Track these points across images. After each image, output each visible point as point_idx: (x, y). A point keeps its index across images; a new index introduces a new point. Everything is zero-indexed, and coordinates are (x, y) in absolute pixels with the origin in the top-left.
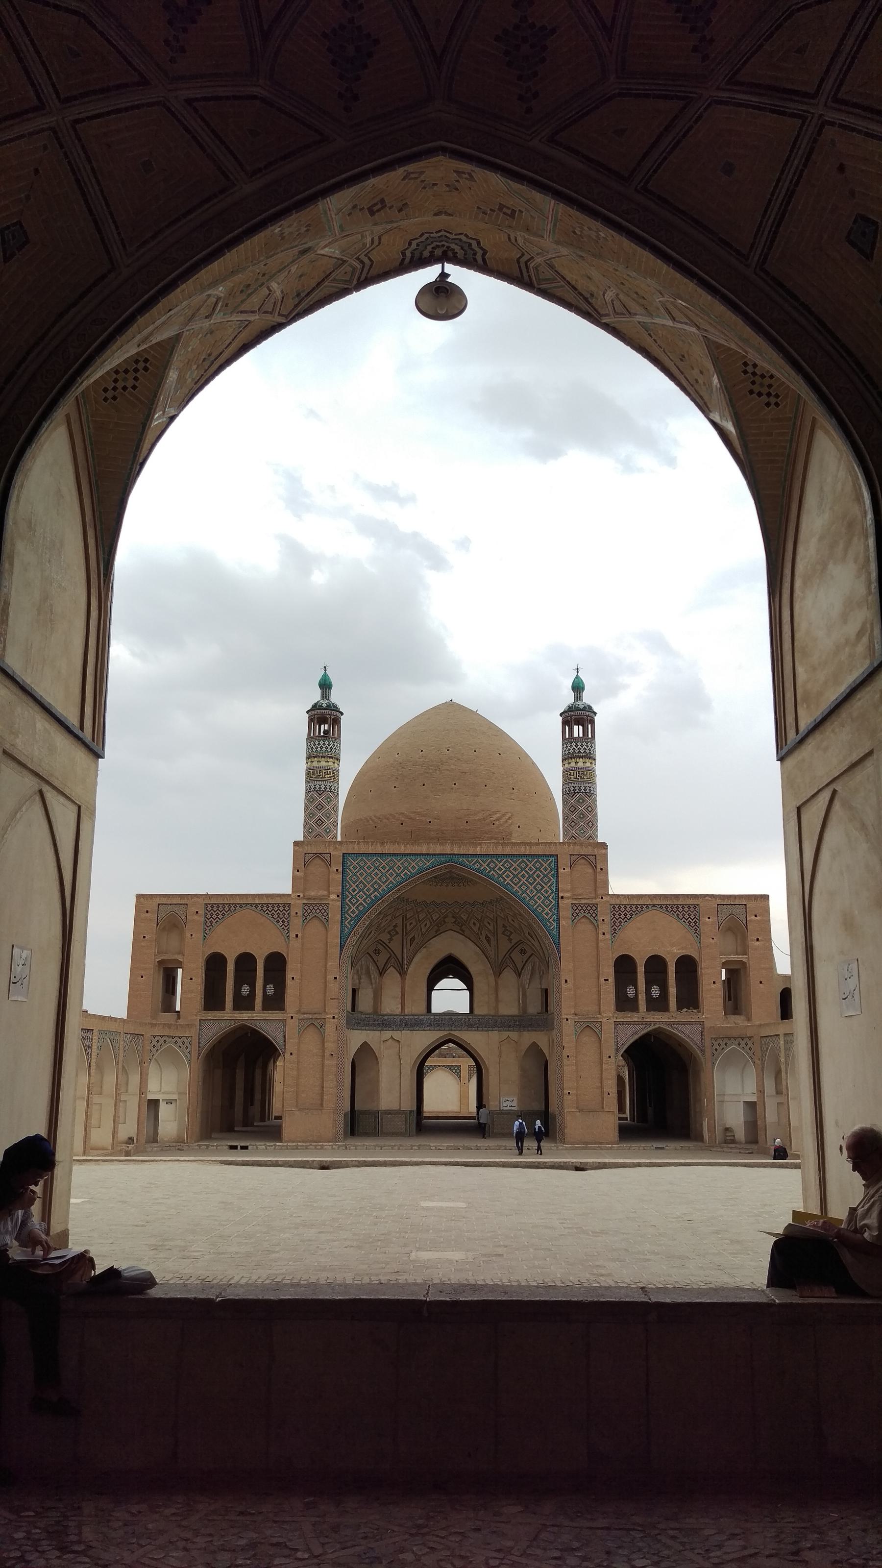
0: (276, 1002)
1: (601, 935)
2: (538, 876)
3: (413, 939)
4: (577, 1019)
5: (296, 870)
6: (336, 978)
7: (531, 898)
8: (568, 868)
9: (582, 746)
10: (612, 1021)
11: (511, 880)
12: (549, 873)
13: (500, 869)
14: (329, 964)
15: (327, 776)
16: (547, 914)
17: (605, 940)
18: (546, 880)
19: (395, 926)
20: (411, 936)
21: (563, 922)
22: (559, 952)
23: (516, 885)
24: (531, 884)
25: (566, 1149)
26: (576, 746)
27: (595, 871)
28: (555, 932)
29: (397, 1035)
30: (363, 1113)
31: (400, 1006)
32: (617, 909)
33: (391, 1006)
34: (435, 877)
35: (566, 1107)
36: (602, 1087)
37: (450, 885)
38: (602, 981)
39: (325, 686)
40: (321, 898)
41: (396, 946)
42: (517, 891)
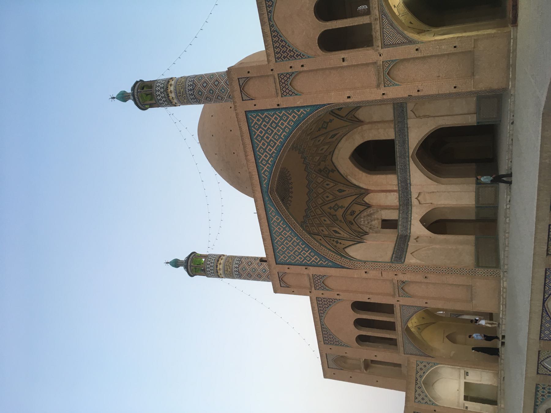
0: (388, 309)
1: (305, 68)
2: (265, 126)
3: (340, 191)
4: (382, 86)
5: (293, 293)
6: (366, 272)
7: (284, 130)
8: (254, 102)
9: (159, 95)
10: (381, 51)
11: (273, 147)
12: (260, 117)
13: (266, 156)
14: (356, 276)
15: (229, 270)
16: (294, 117)
17: (309, 65)
18: (267, 119)
19: (330, 208)
20: (337, 193)
21: (298, 104)
22: (324, 105)
23: (275, 143)
24: (273, 131)
25: (514, 86)
26: (161, 100)
27: (252, 78)
28: (308, 110)
29: (414, 195)
30: (477, 214)
31: (392, 193)
32: (279, 55)
33: (393, 199)
34: (282, 200)
35: (469, 90)
36: (448, 55)
37: (290, 181)
38: (345, 64)
39: (176, 263)
40: (310, 279)
41: (346, 202)
42: (280, 142)
